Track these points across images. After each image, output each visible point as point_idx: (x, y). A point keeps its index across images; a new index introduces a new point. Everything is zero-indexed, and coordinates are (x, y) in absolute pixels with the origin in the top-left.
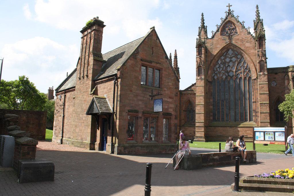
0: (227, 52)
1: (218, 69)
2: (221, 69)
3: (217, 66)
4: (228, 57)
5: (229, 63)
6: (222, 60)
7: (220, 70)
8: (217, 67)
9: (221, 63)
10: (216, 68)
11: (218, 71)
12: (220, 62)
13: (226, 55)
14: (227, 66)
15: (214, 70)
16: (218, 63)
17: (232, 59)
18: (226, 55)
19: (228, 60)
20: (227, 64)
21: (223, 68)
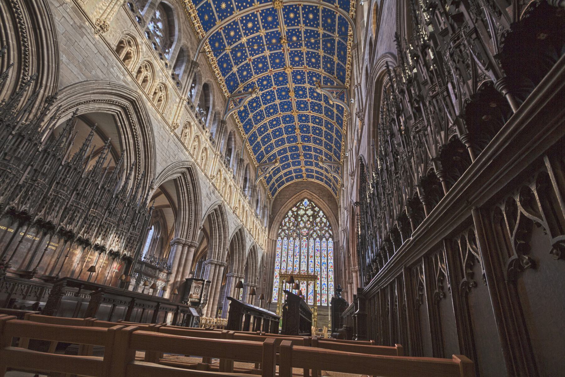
0: (302, 203)
1: (287, 224)
2: (291, 224)
3: (287, 220)
4: (301, 208)
5: (302, 216)
6: (293, 212)
7: (289, 225)
8: (286, 221)
9: (292, 216)
10: (285, 223)
11: (287, 226)
12: (290, 213)
13: (300, 205)
14: (300, 221)
15: (281, 224)
16: (288, 216)
17: (307, 212)
18: (300, 205)
19: (301, 212)
20: (299, 217)
21: (293, 223)
